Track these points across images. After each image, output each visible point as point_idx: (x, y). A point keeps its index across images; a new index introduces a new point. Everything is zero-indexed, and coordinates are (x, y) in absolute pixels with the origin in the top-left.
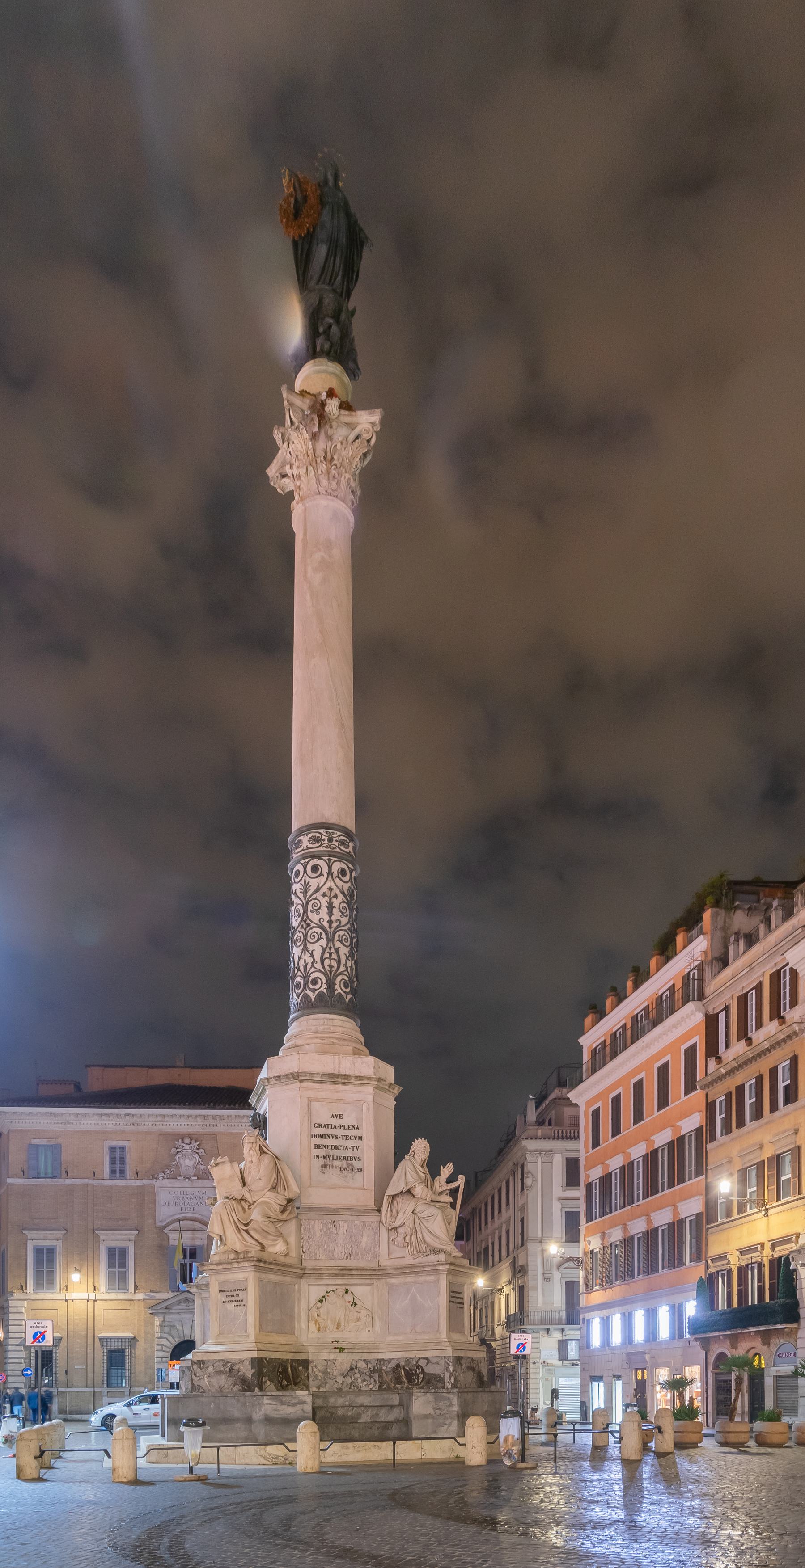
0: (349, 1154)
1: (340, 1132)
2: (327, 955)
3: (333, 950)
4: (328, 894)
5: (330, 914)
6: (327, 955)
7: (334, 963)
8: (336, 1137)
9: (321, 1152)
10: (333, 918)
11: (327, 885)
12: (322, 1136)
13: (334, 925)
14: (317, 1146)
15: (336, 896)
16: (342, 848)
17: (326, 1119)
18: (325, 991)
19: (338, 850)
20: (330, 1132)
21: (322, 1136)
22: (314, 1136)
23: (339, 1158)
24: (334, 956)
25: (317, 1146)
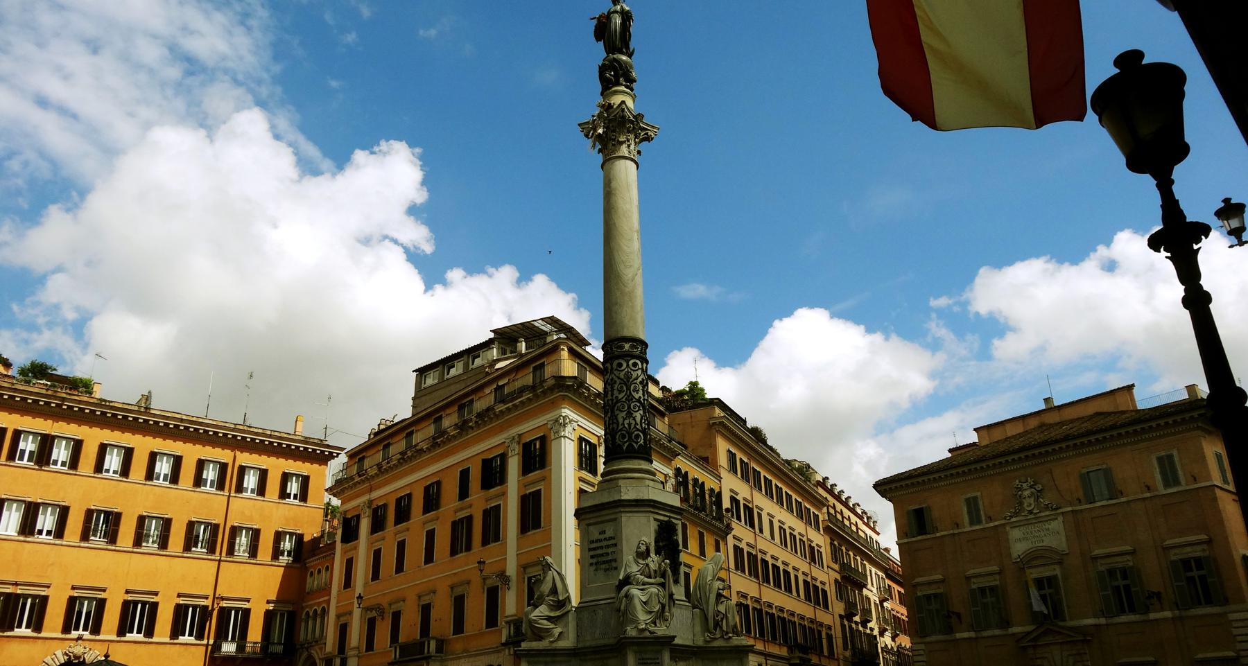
0: (610, 558)
1: (605, 543)
8: (602, 547)
9: (594, 561)
12: (594, 549)
14: (592, 557)
17: (596, 536)
20: (599, 544)
21: (594, 549)
22: (590, 550)
23: (604, 562)
25: (592, 557)
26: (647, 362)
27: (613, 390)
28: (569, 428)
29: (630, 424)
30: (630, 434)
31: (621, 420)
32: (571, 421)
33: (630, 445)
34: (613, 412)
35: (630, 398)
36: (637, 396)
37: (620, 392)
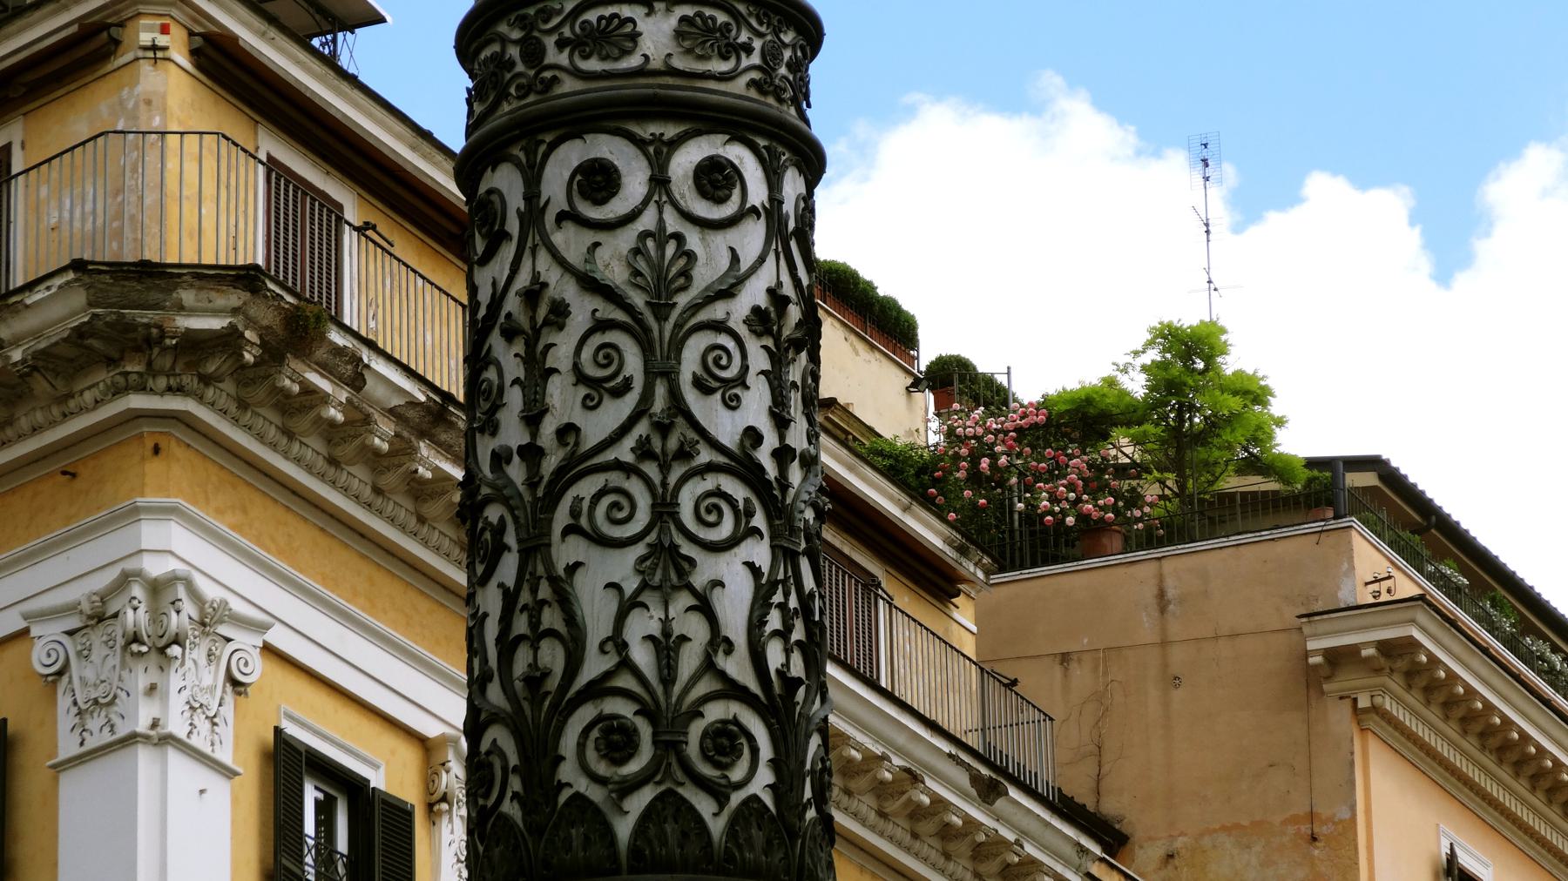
2: (521, 625)
3: (545, 591)
4: (523, 320)
5: (533, 417)
6: (521, 625)
7: (552, 656)
10: (549, 427)
11: (523, 280)
13: (550, 464)
15: (560, 312)
16: (593, 65)
18: (768, 800)
19: (569, 85)
24: (551, 618)
26: (812, 163)
27: (538, 372)
28: (194, 674)
29: (666, 646)
30: (668, 722)
31: (597, 614)
32: (210, 619)
33: (669, 807)
34: (535, 547)
35: (670, 437)
36: (726, 427)
37: (597, 390)
